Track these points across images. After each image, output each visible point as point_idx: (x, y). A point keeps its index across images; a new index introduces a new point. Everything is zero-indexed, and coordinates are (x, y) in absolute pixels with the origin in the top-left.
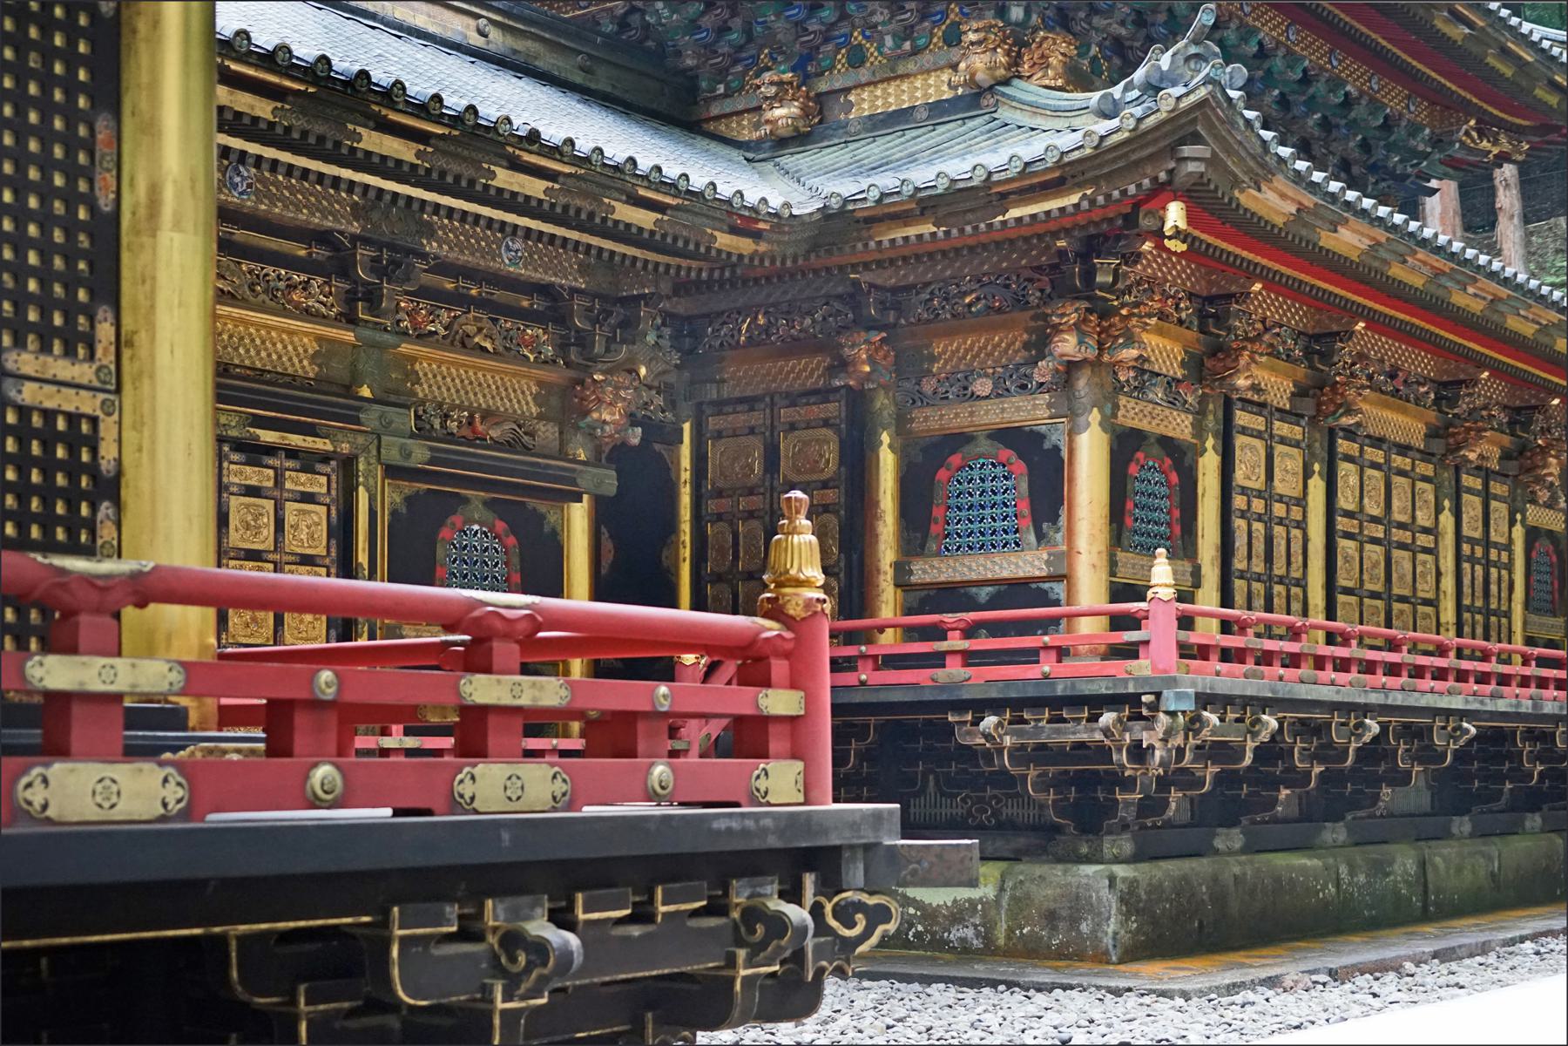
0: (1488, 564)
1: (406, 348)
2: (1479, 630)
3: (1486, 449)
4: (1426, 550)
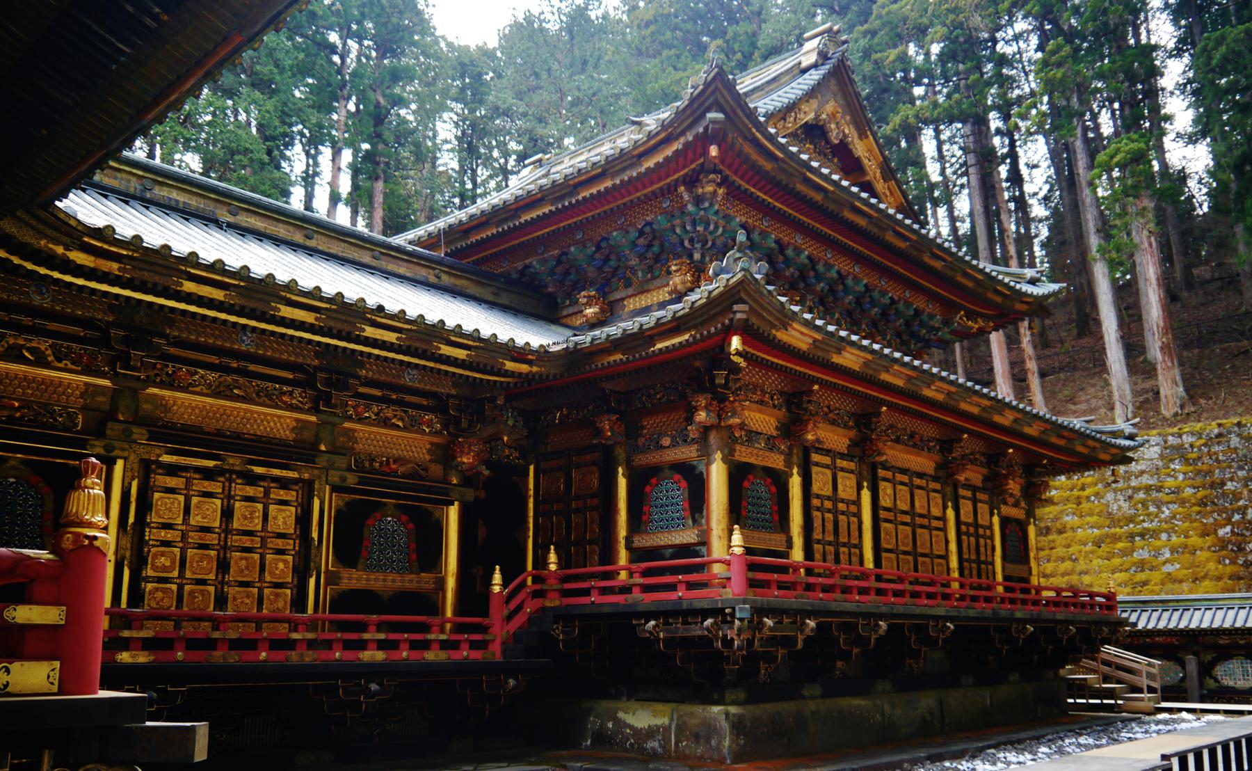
0: (977, 537)
1: (347, 425)
2: (974, 572)
3: (972, 475)
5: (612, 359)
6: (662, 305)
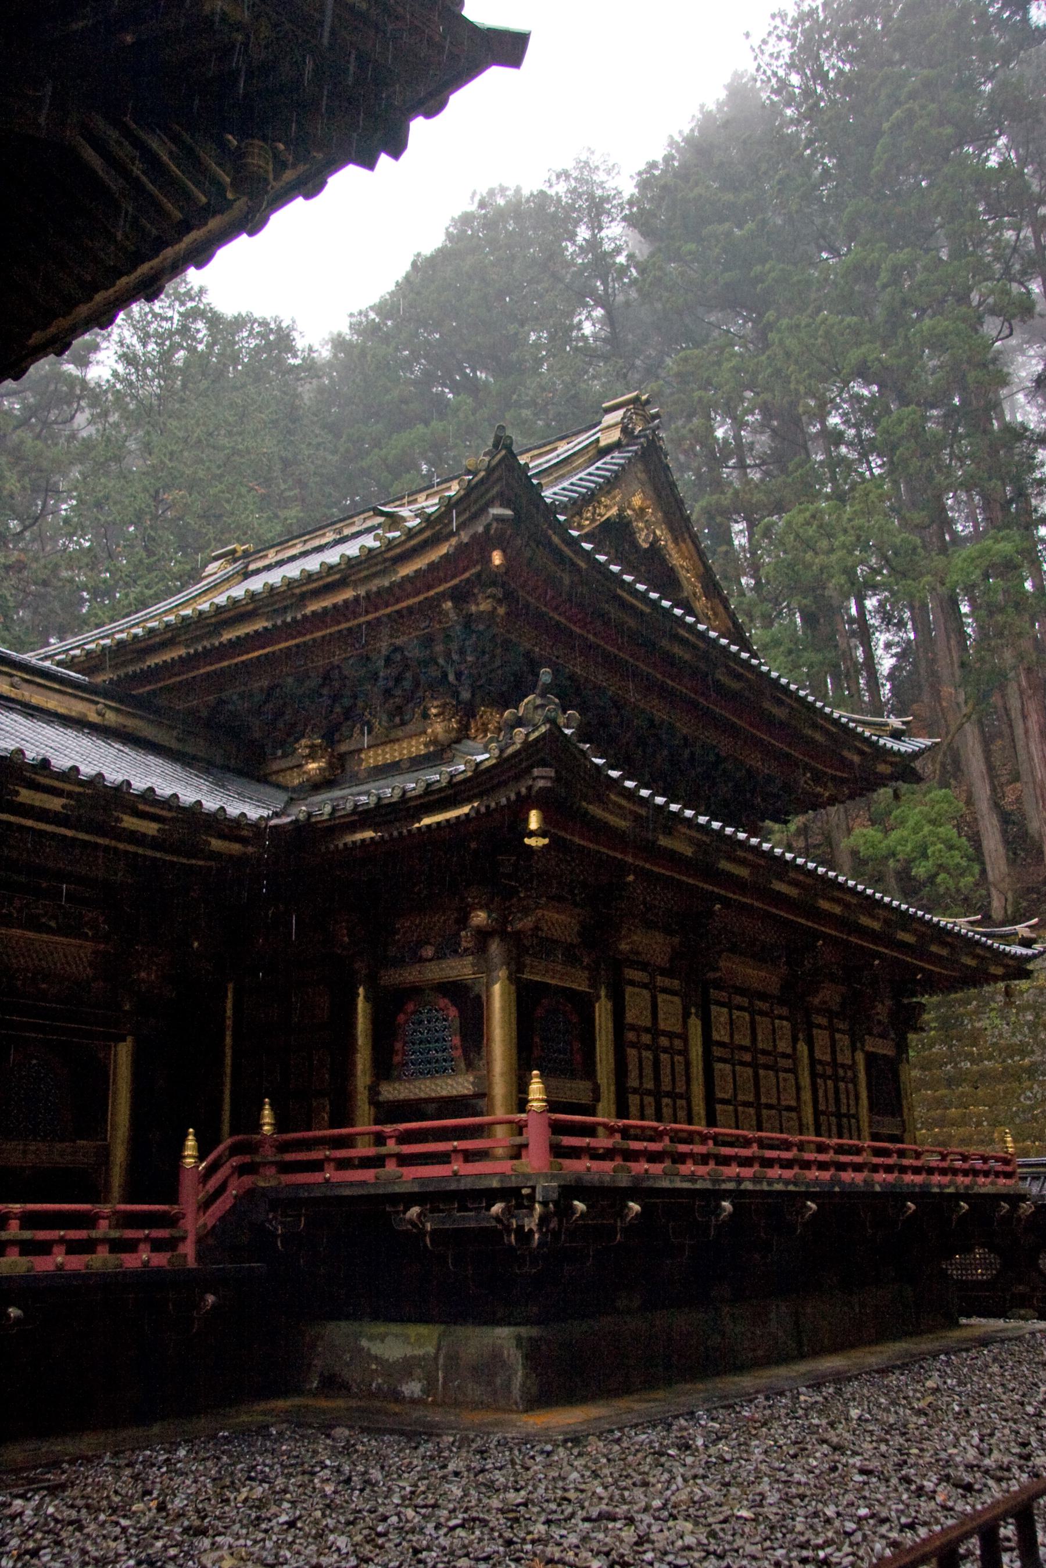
3: (829, 995)
4: (786, 1071)
5: (359, 836)
6: (418, 763)
